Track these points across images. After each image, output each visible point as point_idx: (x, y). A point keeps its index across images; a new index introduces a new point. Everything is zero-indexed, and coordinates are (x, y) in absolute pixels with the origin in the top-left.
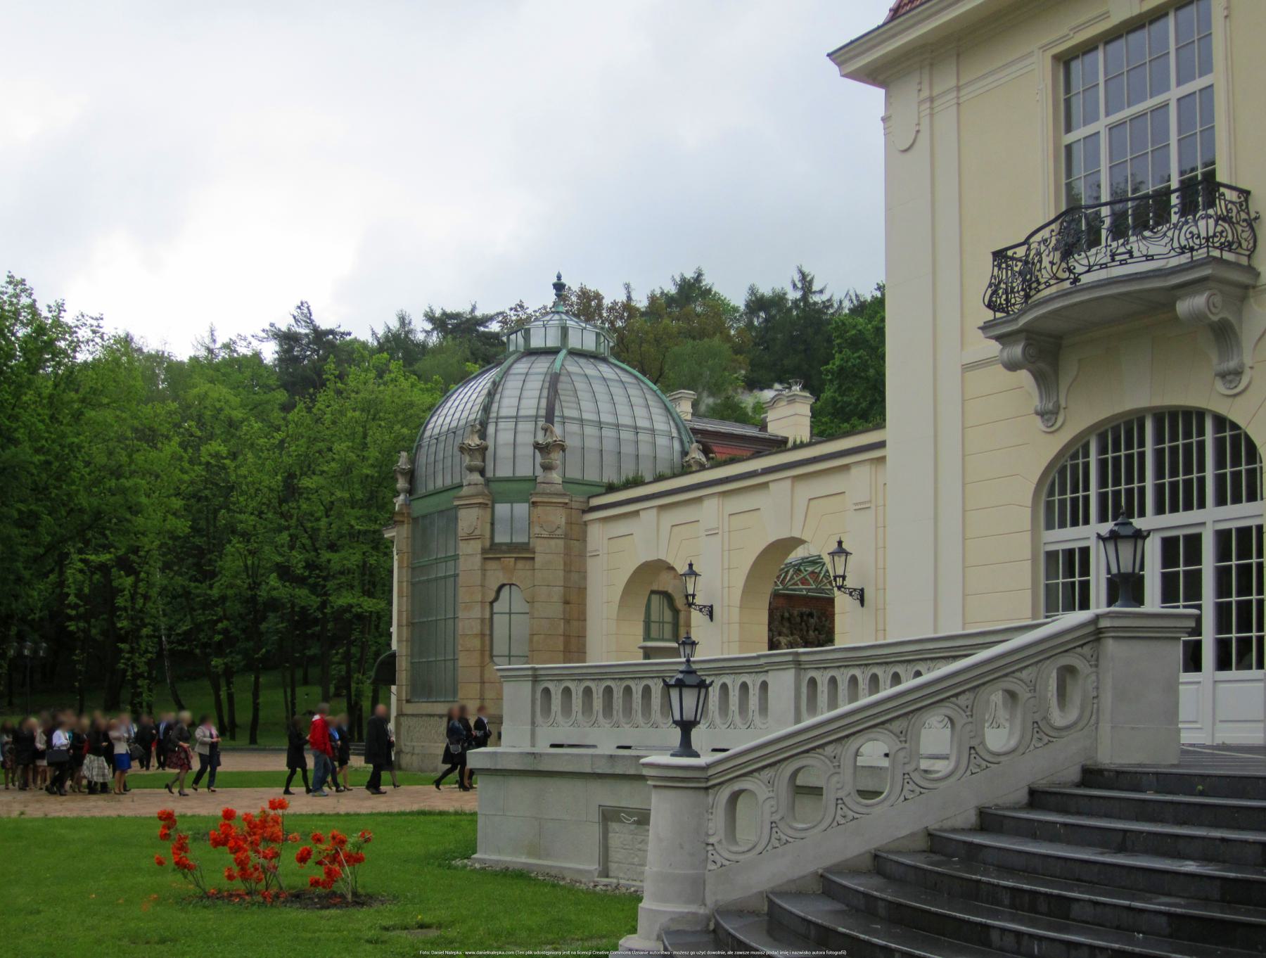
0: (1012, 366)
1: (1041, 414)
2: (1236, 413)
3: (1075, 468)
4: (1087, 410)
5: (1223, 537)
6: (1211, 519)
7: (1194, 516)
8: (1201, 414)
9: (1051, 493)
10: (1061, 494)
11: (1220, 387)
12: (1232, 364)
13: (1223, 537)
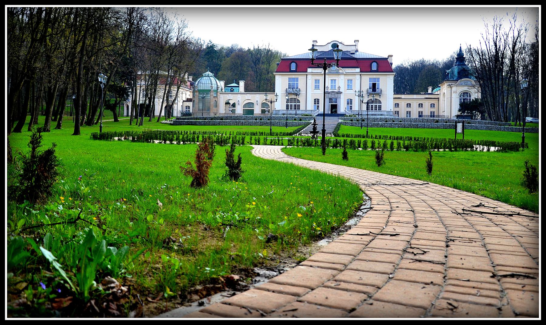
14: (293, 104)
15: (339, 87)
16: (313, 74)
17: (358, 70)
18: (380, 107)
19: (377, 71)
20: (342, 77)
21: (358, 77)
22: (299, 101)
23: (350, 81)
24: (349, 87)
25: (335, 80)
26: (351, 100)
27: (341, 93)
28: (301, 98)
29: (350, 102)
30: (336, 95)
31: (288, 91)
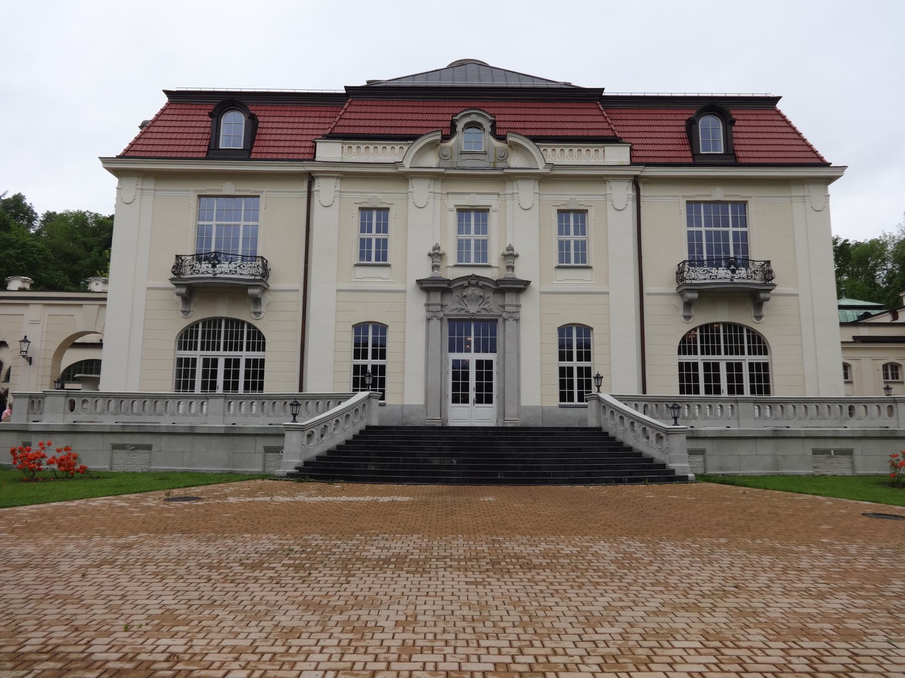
0: (178, 294)
1: (183, 312)
2: (259, 325)
3: (192, 331)
4: (200, 313)
5: (248, 361)
6: (244, 355)
7: (238, 353)
8: (243, 322)
9: (181, 338)
10: (186, 339)
11: (253, 316)
12: (259, 310)
13: (248, 361)
14: (222, 355)
15: (510, 256)
16: (348, 175)
17: (618, 155)
18: (761, 378)
19: (730, 158)
20: (527, 192)
21: (622, 193)
22: (258, 341)
23: (573, 218)
24: (574, 257)
25: (483, 211)
26: (585, 330)
27: (520, 287)
28: (276, 322)
29: (575, 343)
30: (493, 305)
31: (188, 273)
